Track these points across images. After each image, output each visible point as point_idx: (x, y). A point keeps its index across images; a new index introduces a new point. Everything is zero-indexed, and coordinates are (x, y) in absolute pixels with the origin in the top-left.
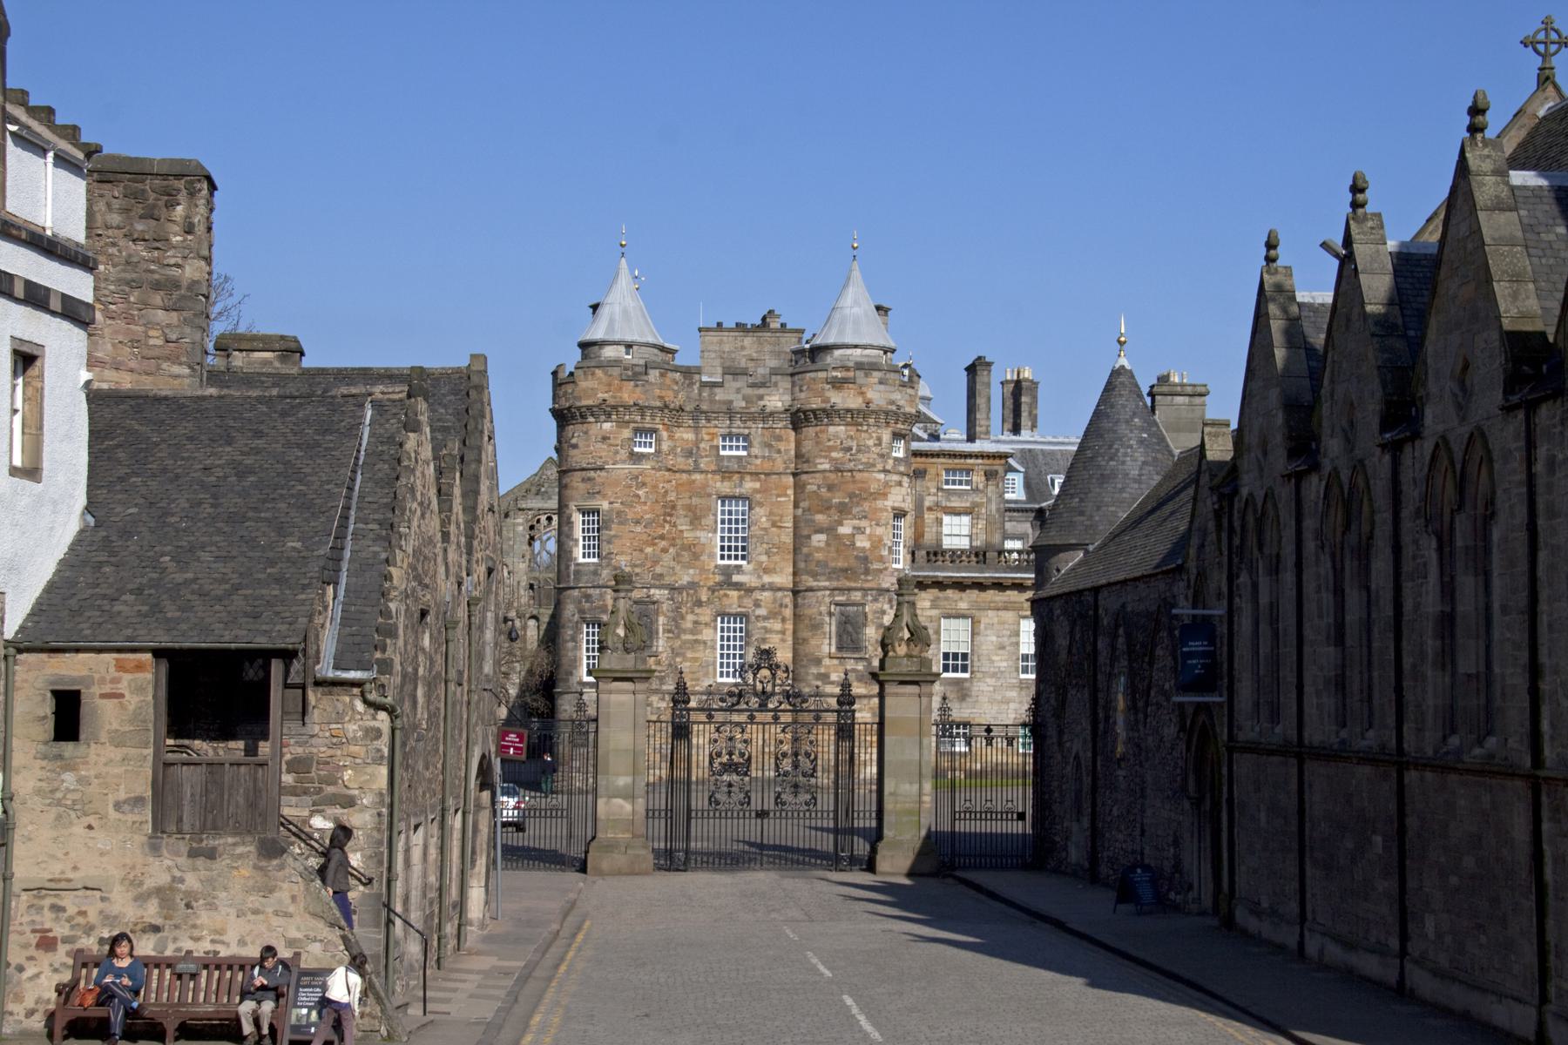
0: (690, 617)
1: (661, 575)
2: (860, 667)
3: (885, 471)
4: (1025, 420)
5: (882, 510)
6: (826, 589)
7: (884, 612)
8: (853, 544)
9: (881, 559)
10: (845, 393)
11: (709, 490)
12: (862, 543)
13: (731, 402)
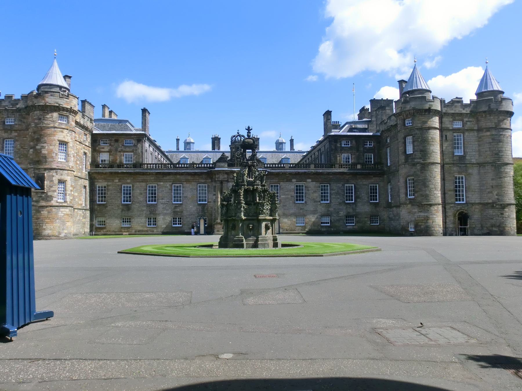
4: (216, 147)
6: (32, 168)
7: (53, 176)
8: (41, 152)
9: (52, 157)
12: (44, 152)
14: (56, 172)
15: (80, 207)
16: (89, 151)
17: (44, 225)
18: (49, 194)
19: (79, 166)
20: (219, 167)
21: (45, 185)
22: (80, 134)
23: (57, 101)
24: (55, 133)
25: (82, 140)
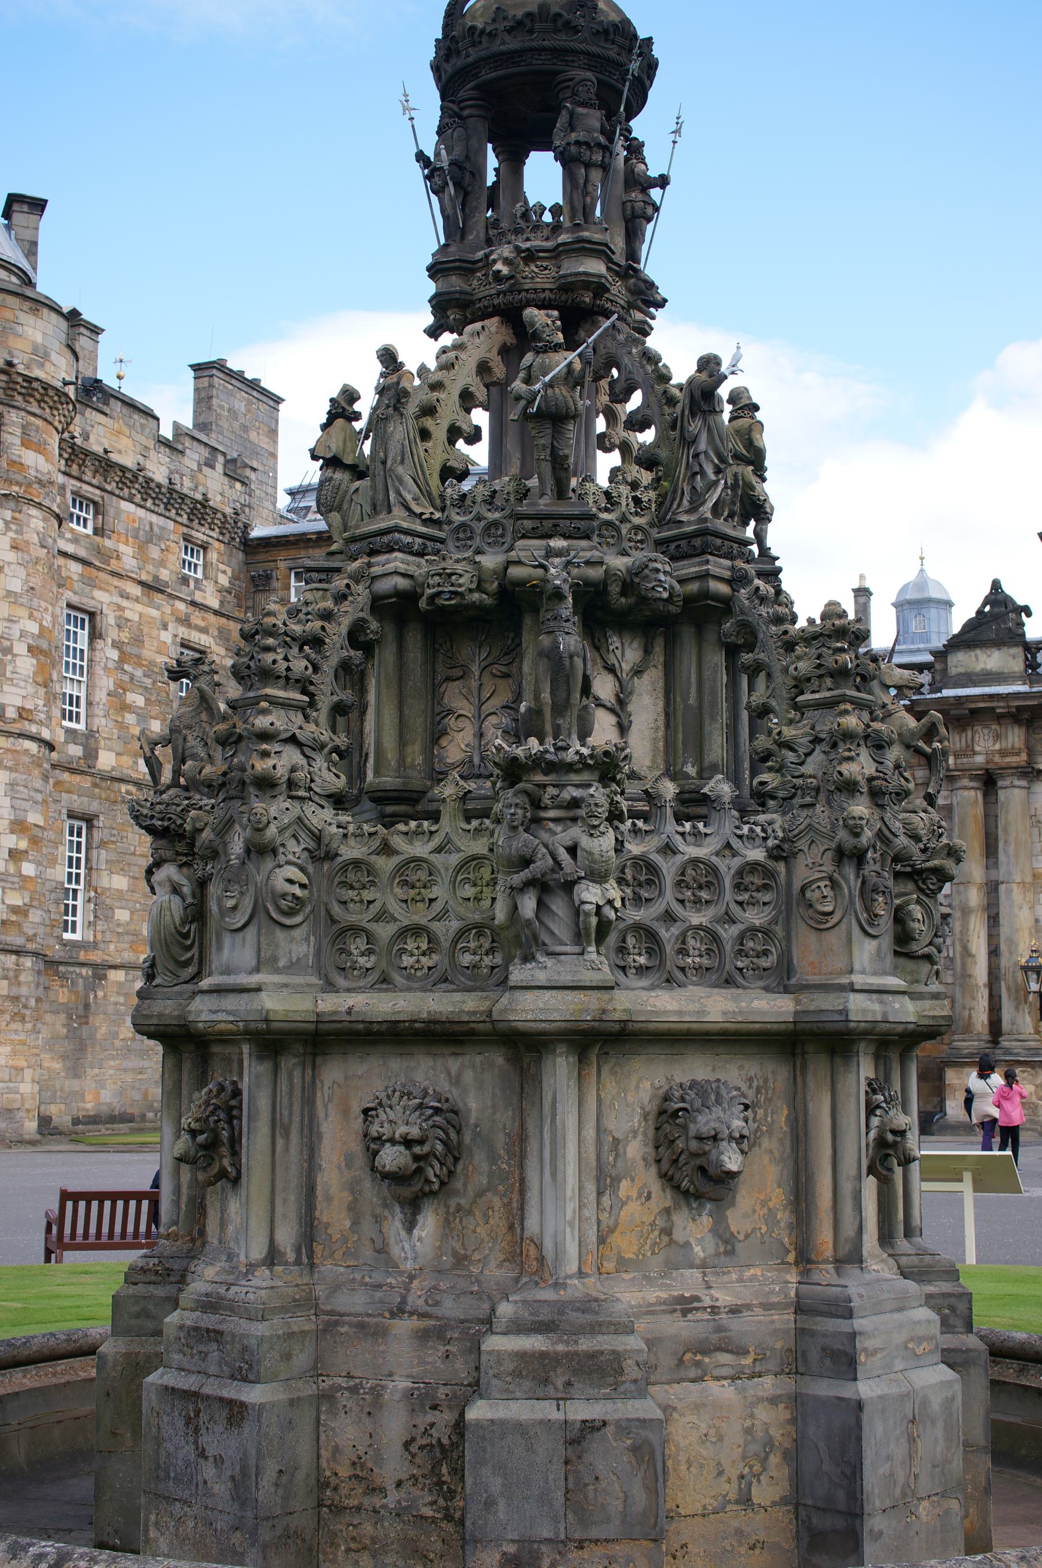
16: (223, 635)
19: (143, 717)
20: (969, 679)
22: (145, 539)
25: (165, 575)
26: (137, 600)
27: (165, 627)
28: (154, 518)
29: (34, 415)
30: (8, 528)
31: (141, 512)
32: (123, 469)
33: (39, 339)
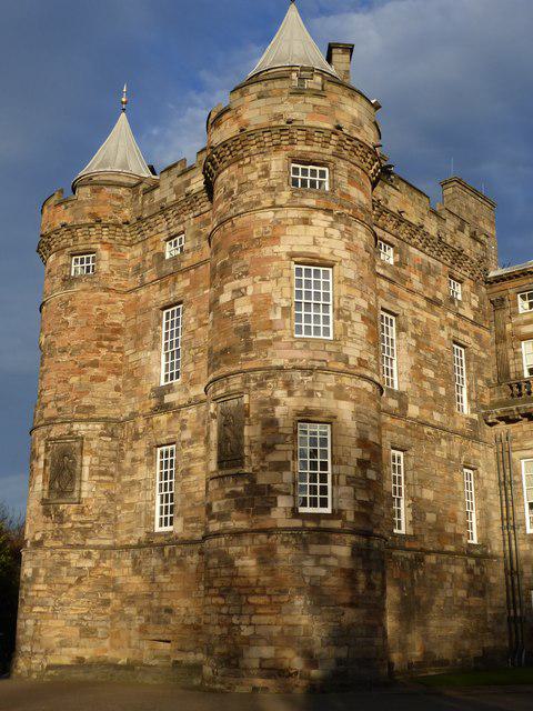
0: (129, 455)
1: (91, 408)
2: (240, 489)
3: (274, 206)
5: (269, 259)
9: (270, 326)
10: (222, 127)
11: (150, 304)
12: (243, 308)
13: (165, 199)
14: (288, 385)
15: (451, 548)
16: (478, 337)
17: (245, 620)
18: (262, 480)
19: (434, 385)
21: (247, 442)
22: (427, 272)
23: (279, 110)
24: (279, 231)
25: (439, 296)
26: (425, 309)
27: (442, 328)
28: (430, 260)
29: (356, 165)
30: (343, 236)
31: (422, 255)
32: (410, 224)
33: (356, 114)
